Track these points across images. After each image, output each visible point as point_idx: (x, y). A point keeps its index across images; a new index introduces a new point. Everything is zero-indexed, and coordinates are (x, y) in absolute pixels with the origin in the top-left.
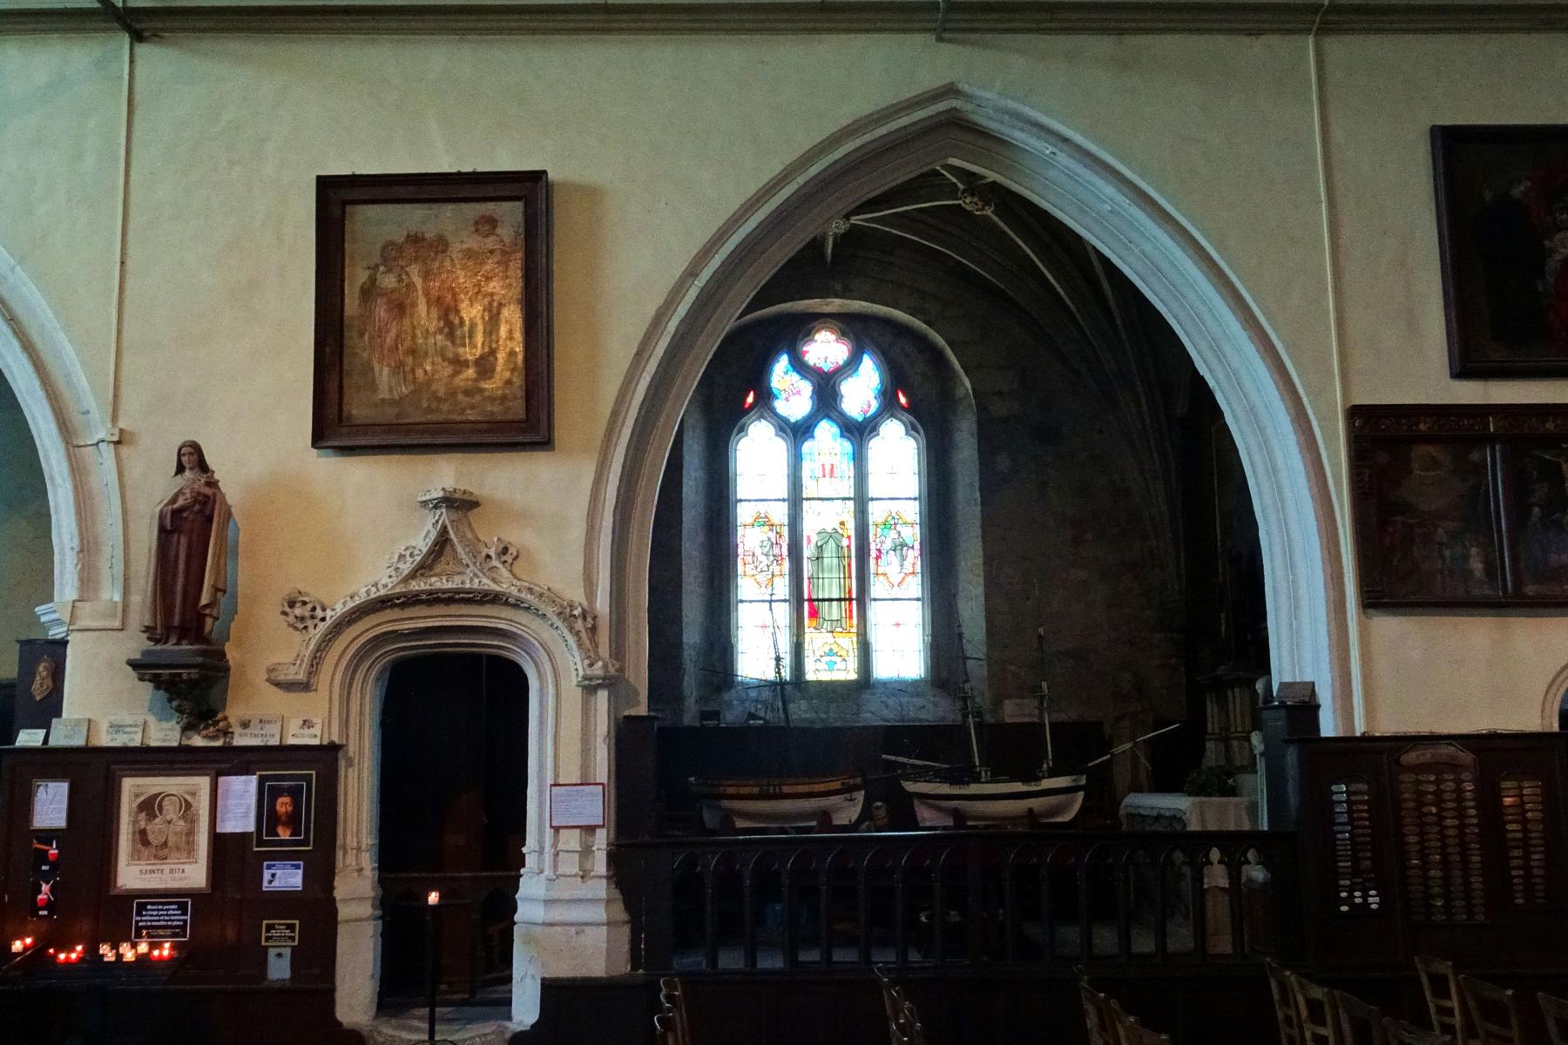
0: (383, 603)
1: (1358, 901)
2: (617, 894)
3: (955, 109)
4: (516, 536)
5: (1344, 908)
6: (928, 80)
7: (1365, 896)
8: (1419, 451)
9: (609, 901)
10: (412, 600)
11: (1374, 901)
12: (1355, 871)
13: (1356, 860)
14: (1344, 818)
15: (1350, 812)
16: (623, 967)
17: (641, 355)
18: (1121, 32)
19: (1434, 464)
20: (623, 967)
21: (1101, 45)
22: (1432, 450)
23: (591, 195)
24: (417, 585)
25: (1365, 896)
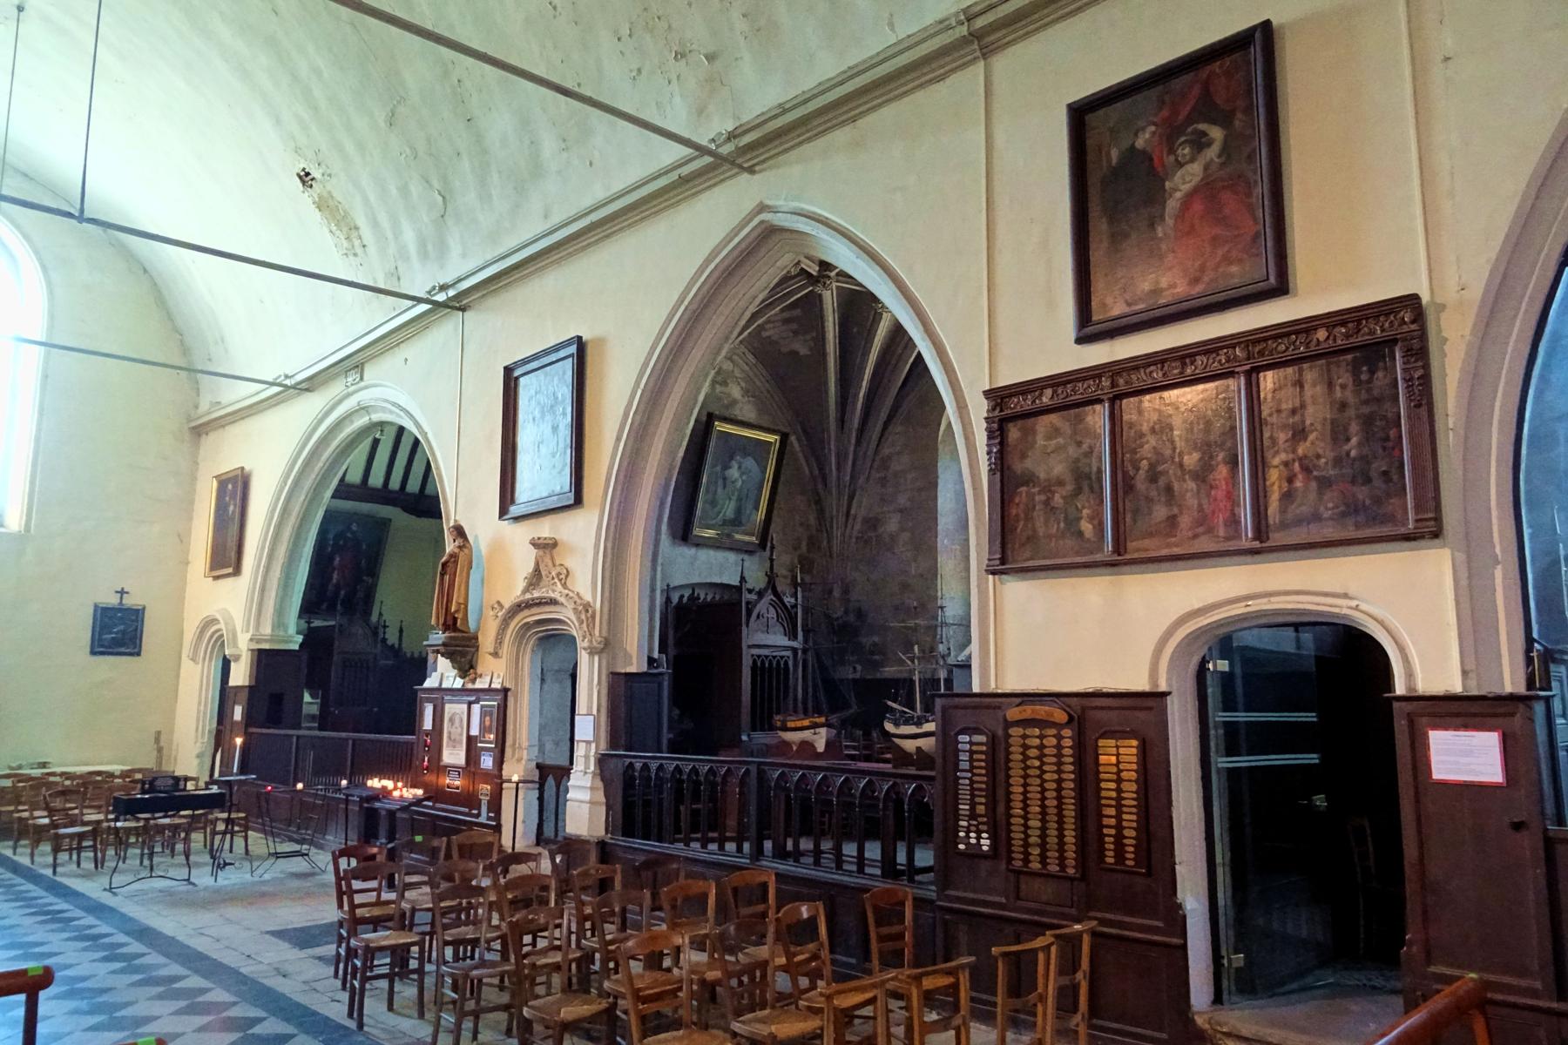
0: (519, 607)
1: (973, 841)
2: (600, 784)
3: (762, 222)
4: (570, 563)
5: (962, 847)
6: (749, 206)
7: (979, 838)
8: (1043, 423)
9: (592, 788)
10: (529, 605)
11: (985, 844)
12: (973, 815)
13: (973, 805)
14: (964, 765)
15: (971, 760)
16: (600, 831)
17: (618, 439)
18: (854, 120)
19: (1055, 432)
20: (600, 831)
21: (841, 136)
22: (1053, 418)
23: (601, 342)
24: (528, 596)
25: (979, 838)
